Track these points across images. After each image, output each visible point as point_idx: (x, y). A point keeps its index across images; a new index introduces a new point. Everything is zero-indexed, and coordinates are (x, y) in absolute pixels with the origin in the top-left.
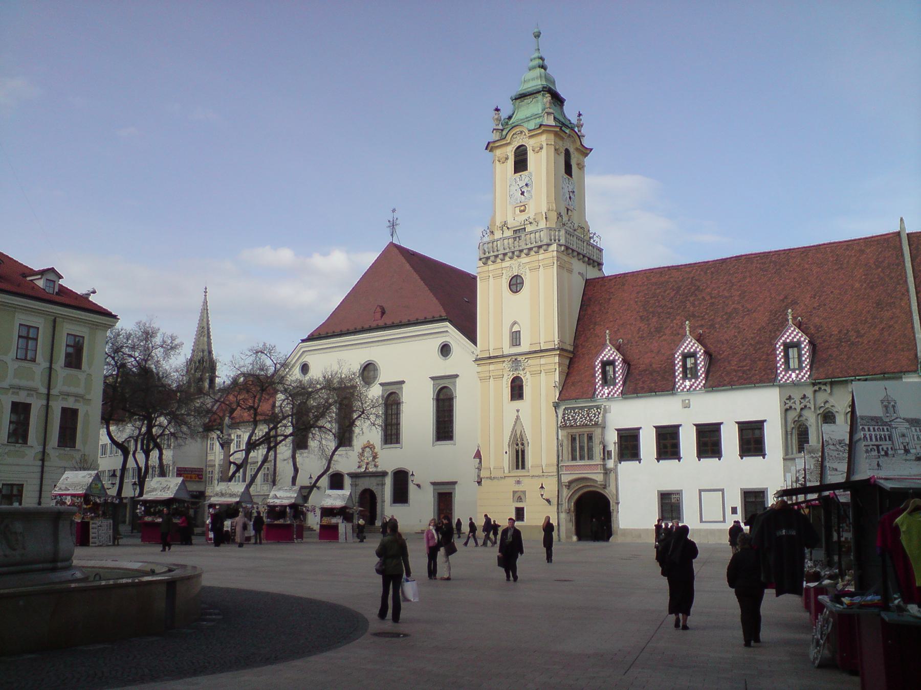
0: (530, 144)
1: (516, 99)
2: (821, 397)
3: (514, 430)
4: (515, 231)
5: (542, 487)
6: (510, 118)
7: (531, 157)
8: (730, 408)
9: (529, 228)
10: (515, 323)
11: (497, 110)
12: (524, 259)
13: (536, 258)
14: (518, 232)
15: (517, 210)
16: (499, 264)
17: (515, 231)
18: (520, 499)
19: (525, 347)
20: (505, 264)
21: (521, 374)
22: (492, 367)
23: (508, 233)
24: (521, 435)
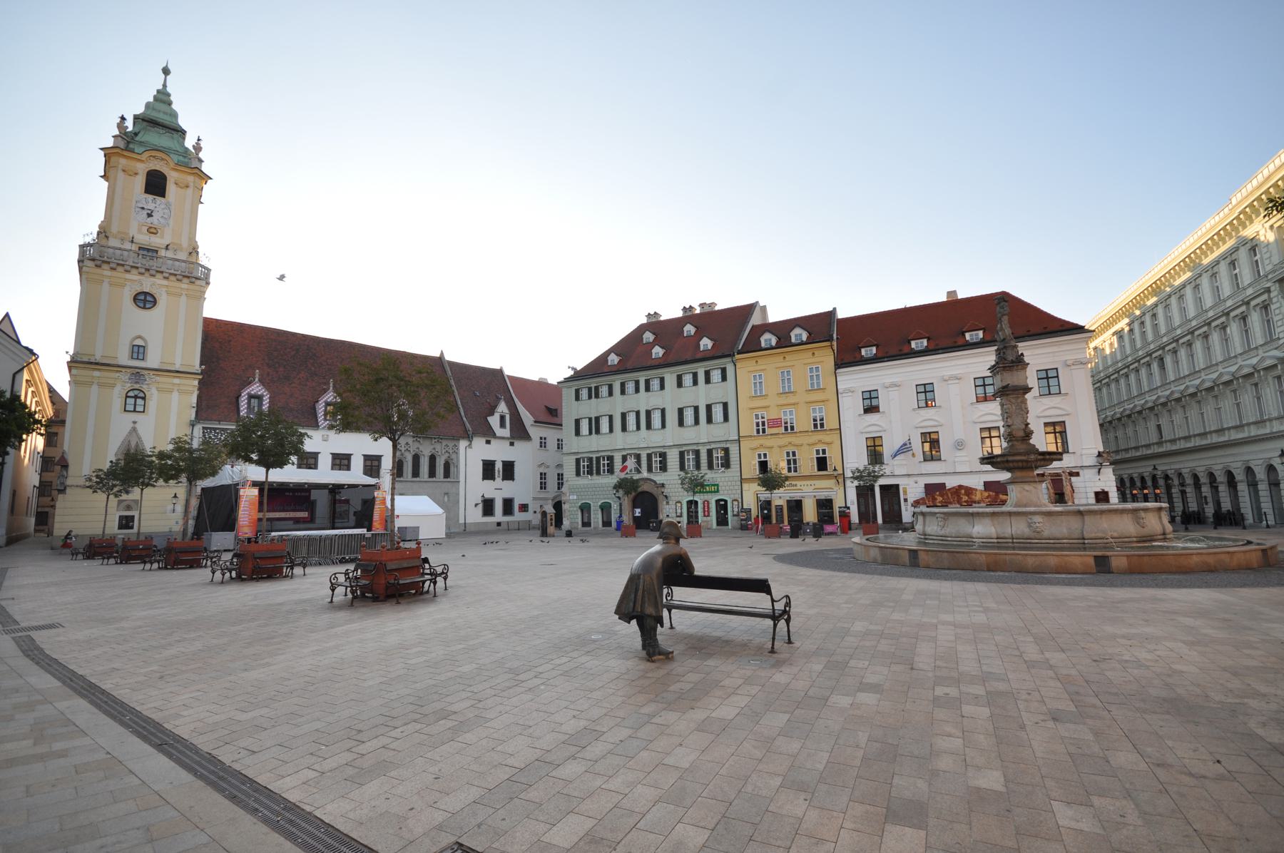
0: (172, 176)
1: (143, 120)
2: (417, 445)
3: (127, 442)
4: (140, 248)
5: (175, 496)
6: (136, 134)
7: (171, 188)
8: (359, 444)
9: (162, 253)
10: (140, 337)
11: (123, 118)
12: (159, 280)
13: (178, 284)
14: (149, 252)
15: (145, 229)
16: (120, 273)
17: (140, 248)
18: (128, 508)
19: (153, 360)
20: (128, 276)
21: (145, 388)
22: (96, 374)
23: (135, 247)
24: (137, 445)
